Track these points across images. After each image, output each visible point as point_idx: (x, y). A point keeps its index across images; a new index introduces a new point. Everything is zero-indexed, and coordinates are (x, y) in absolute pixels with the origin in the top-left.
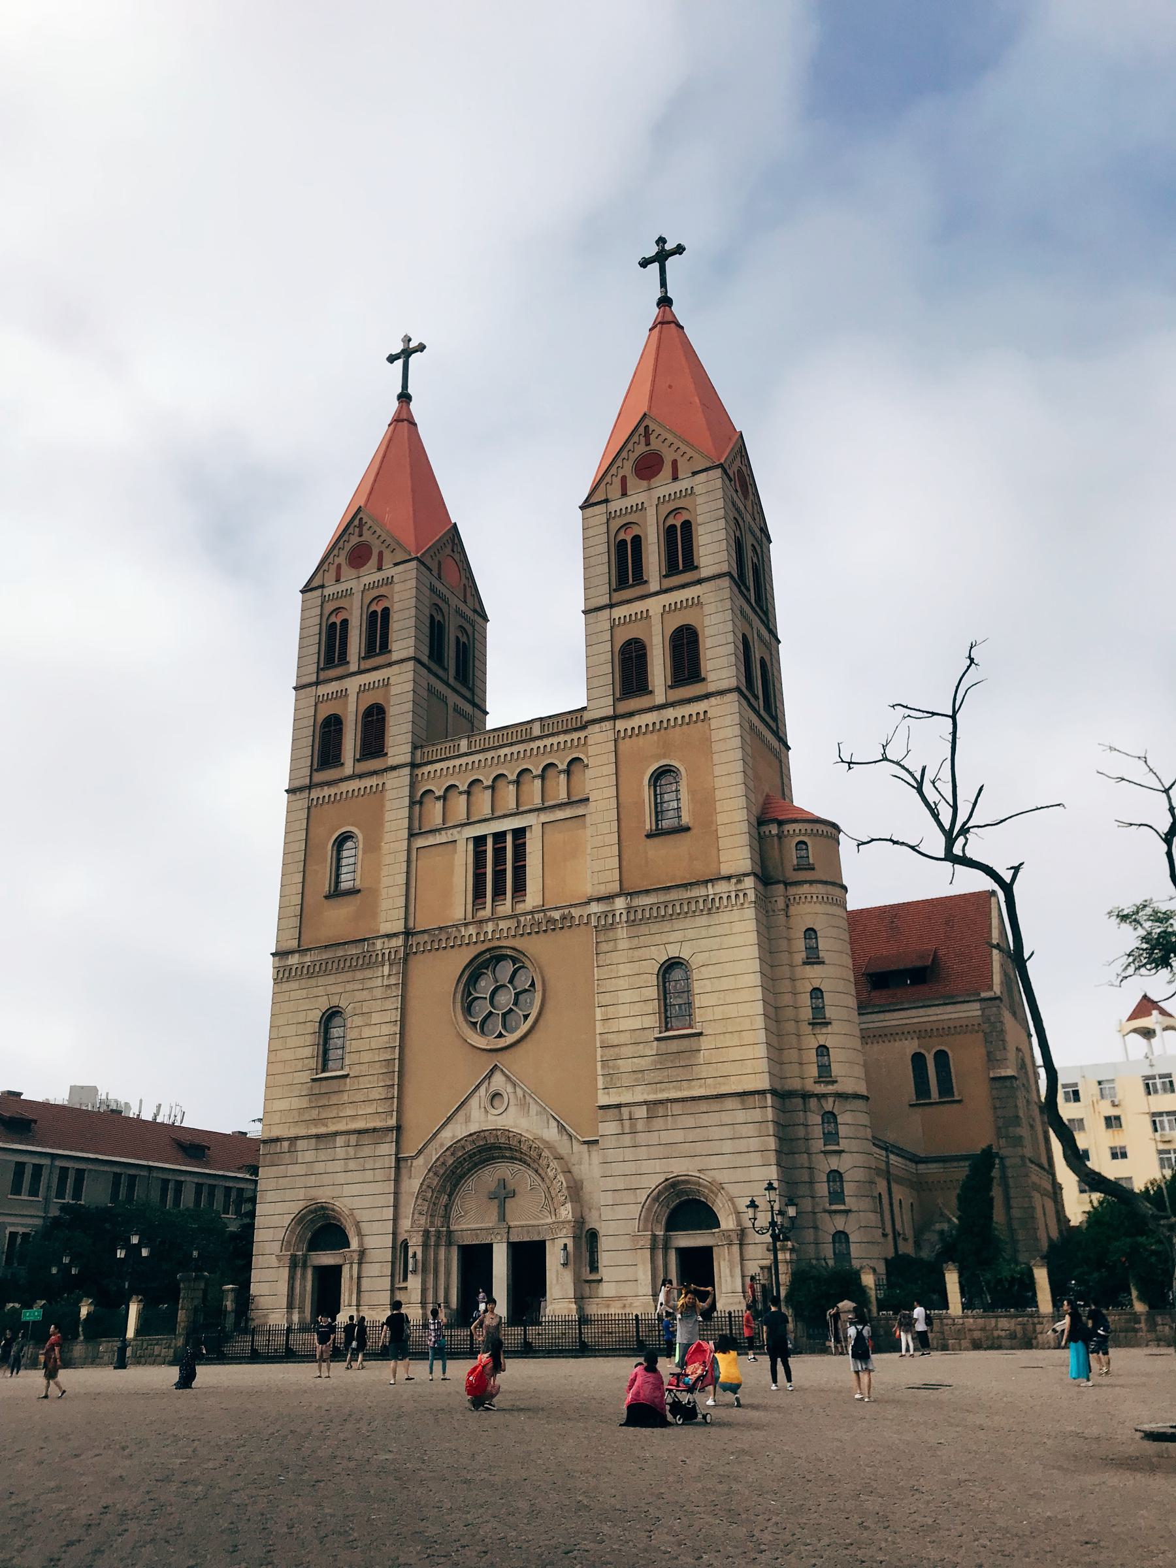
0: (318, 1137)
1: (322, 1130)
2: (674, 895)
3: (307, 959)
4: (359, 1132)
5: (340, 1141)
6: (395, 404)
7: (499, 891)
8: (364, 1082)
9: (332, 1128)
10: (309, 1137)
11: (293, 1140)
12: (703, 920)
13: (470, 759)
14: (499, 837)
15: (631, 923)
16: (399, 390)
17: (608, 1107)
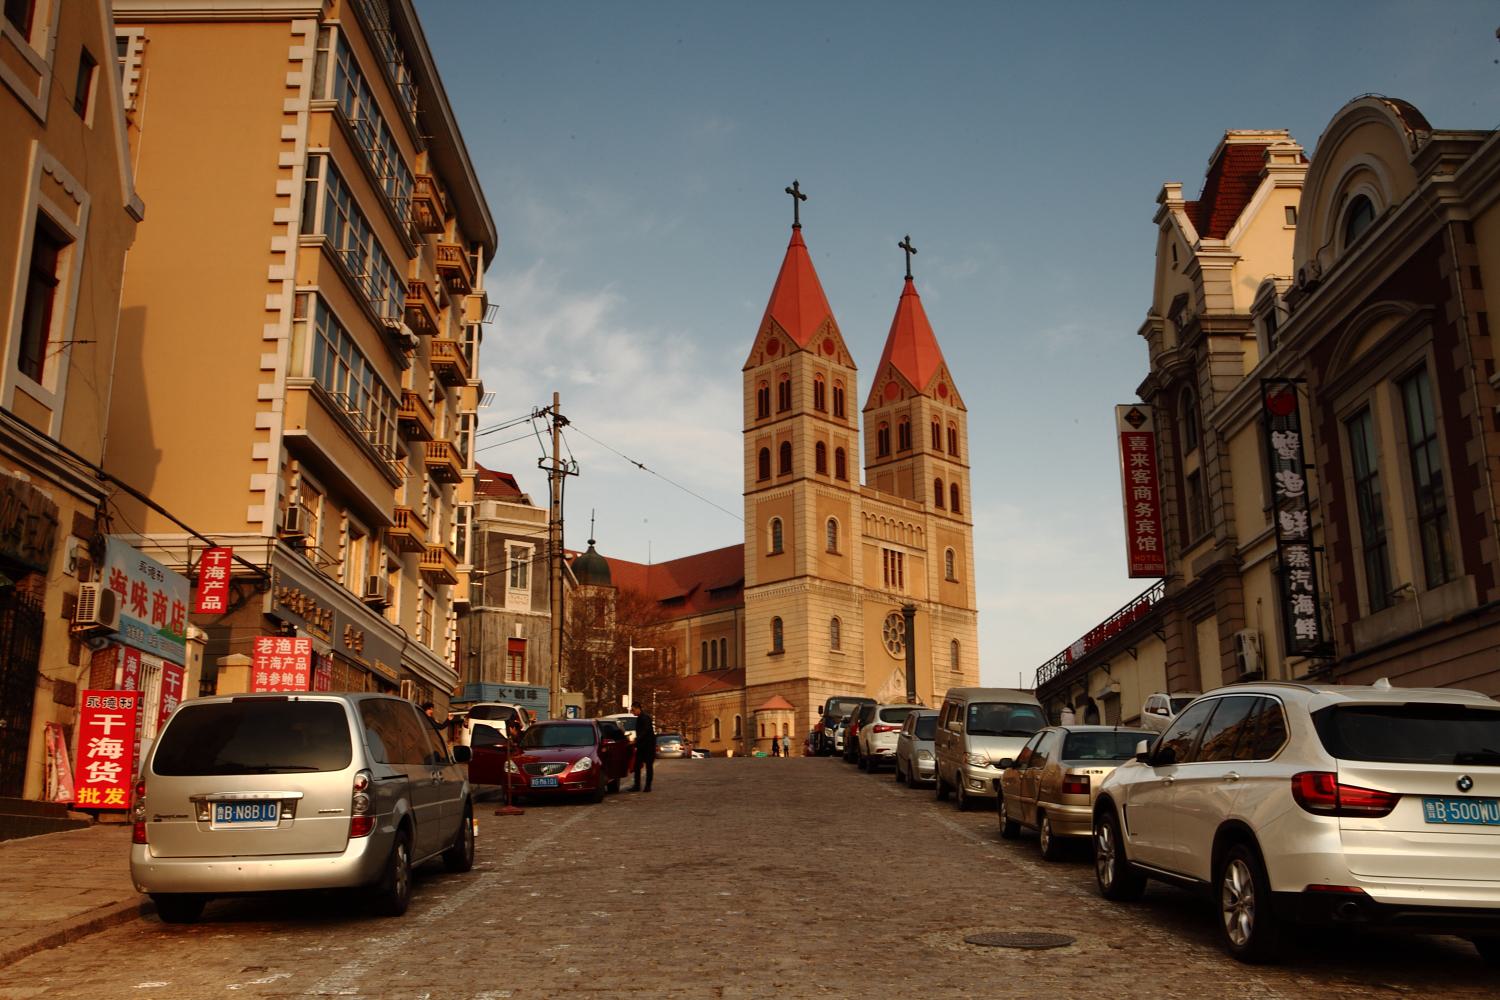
0: (835, 683)
1: (835, 680)
2: (956, 611)
3: (824, 584)
4: (852, 685)
5: (844, 687)
6: (791, 232)
7: (894, 582)
8: (852, 660)
9: (841, 680)
10: (830, 682)
11: (824, 681)
12: (963, 626)
13: (879, 504)
14: (892, 552)
15: (943, 619)
16: (793, 222)
17: (937, 696)
